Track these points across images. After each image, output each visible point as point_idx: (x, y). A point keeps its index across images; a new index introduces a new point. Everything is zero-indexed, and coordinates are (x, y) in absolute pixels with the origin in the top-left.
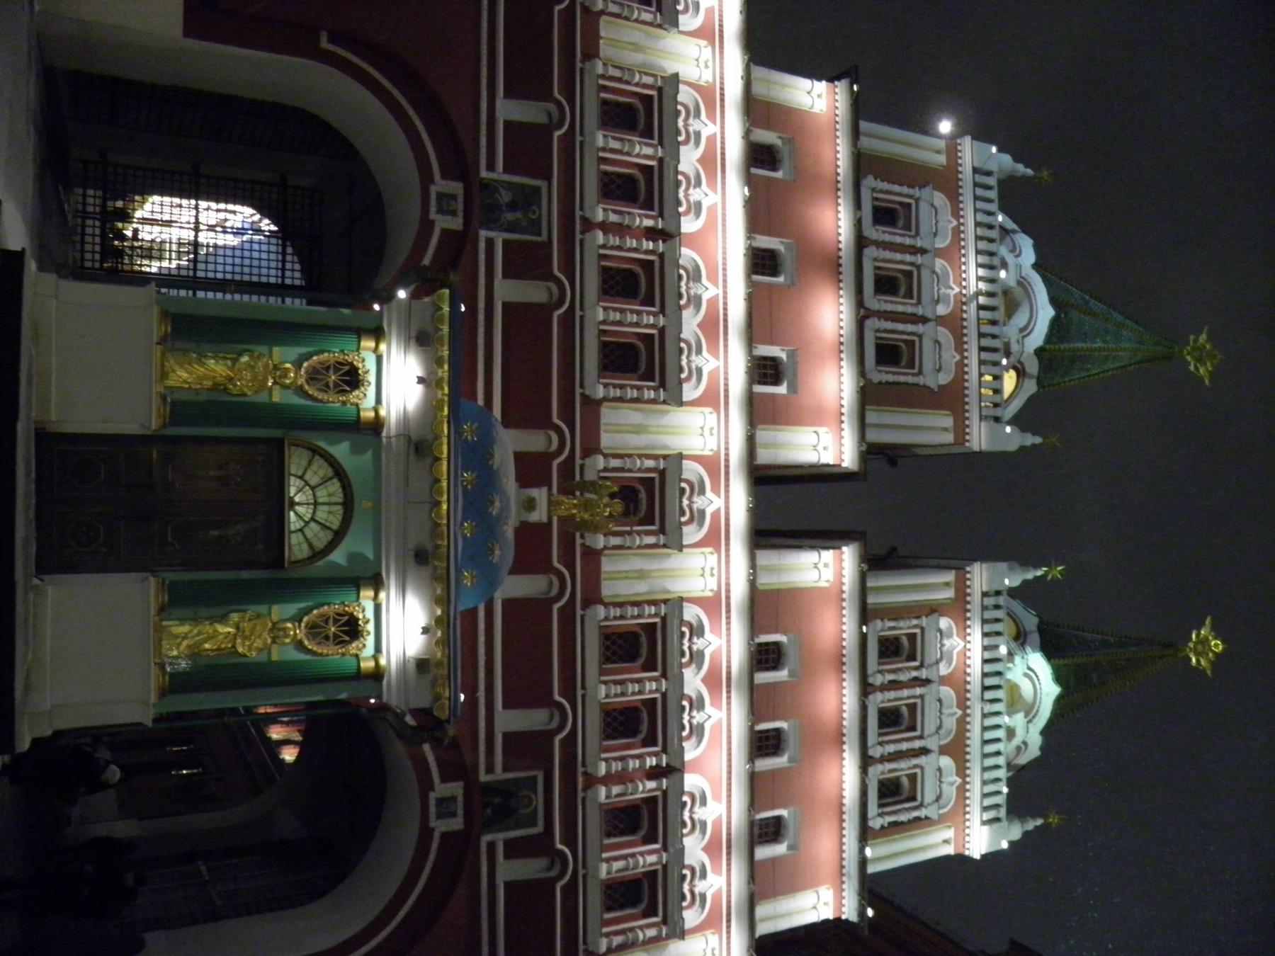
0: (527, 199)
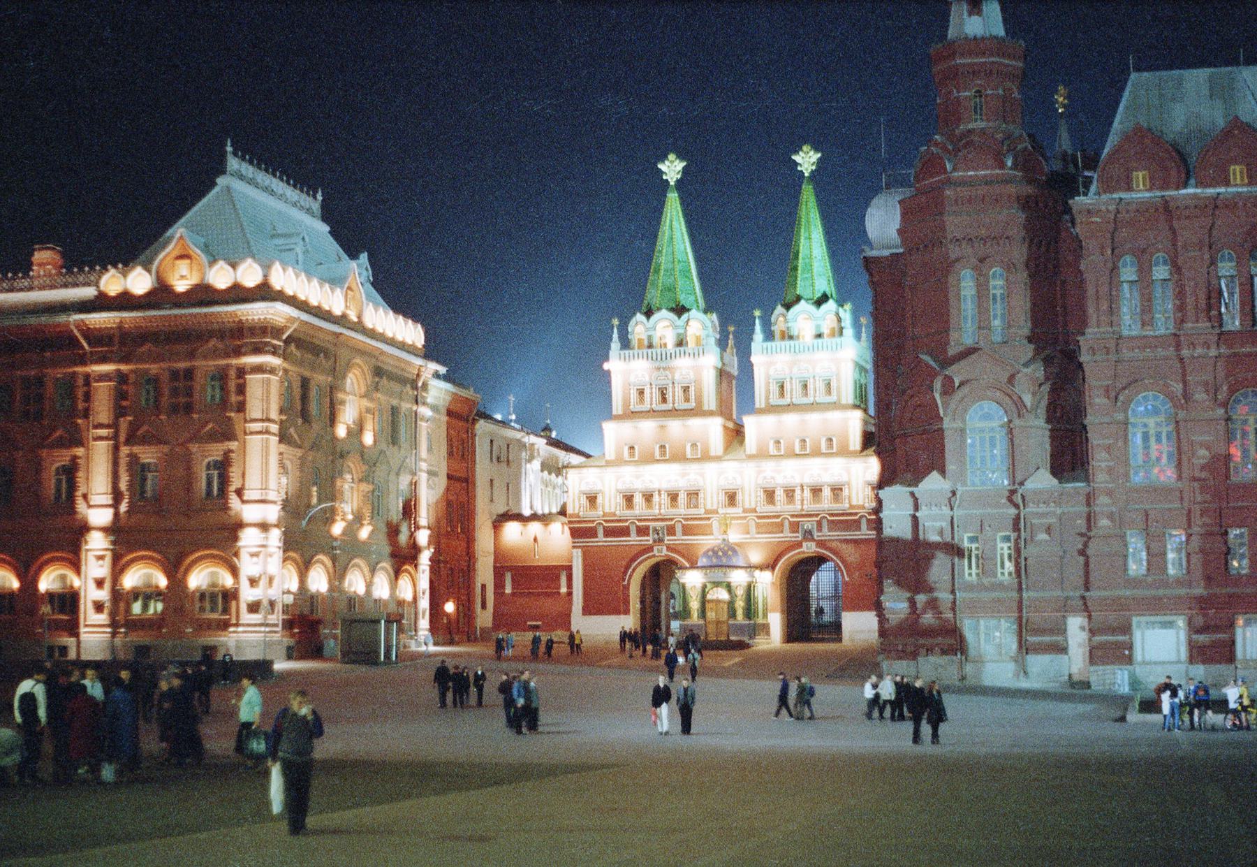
0: (656, 530)
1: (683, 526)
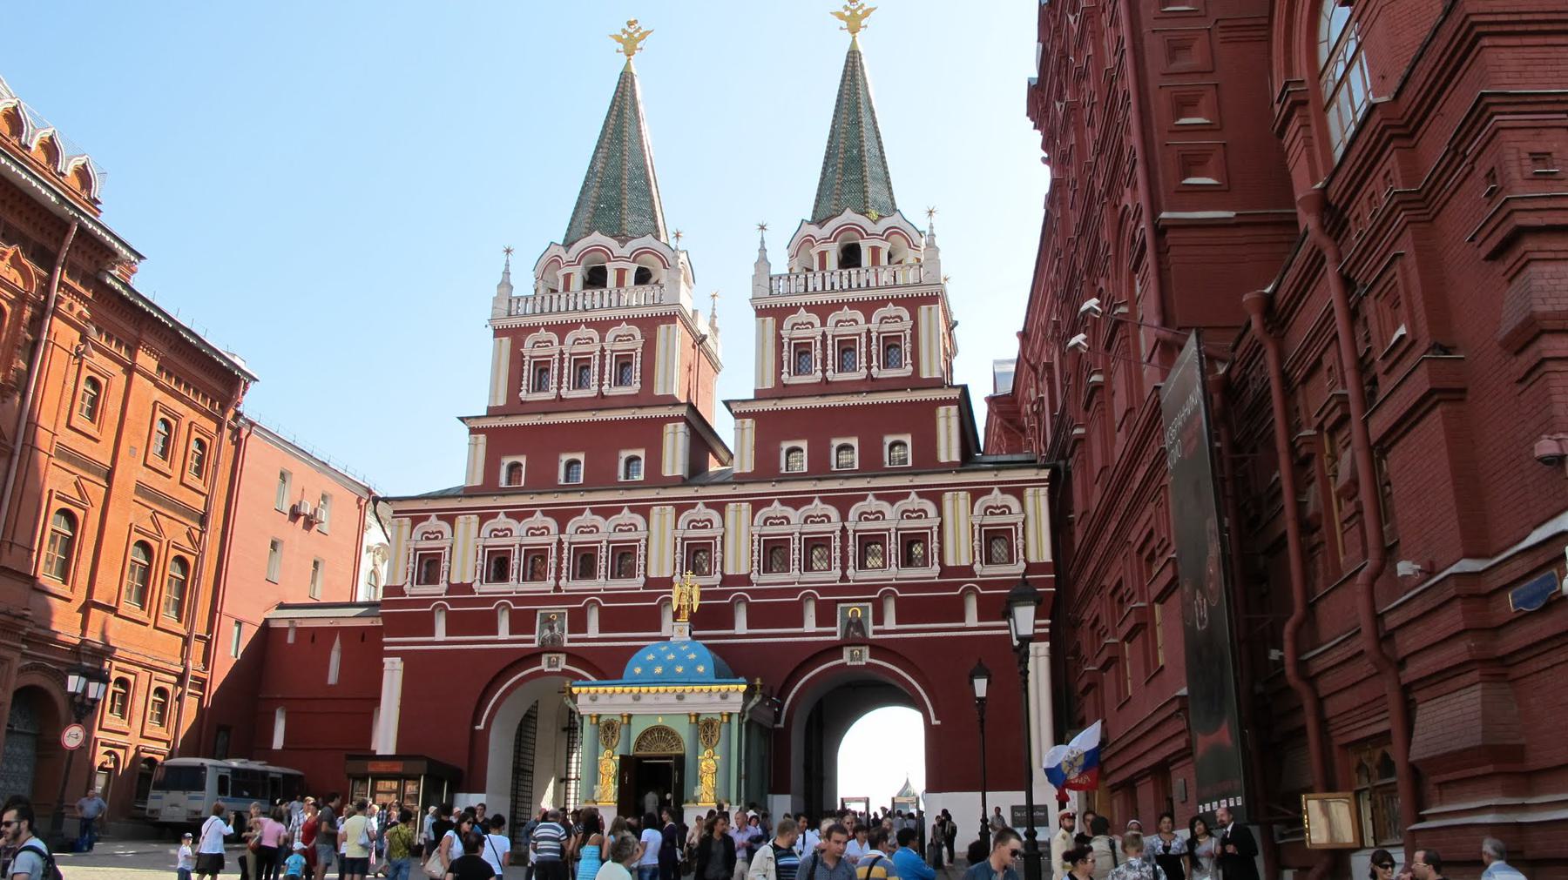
0: (548, 621)
1: (602, 611)
